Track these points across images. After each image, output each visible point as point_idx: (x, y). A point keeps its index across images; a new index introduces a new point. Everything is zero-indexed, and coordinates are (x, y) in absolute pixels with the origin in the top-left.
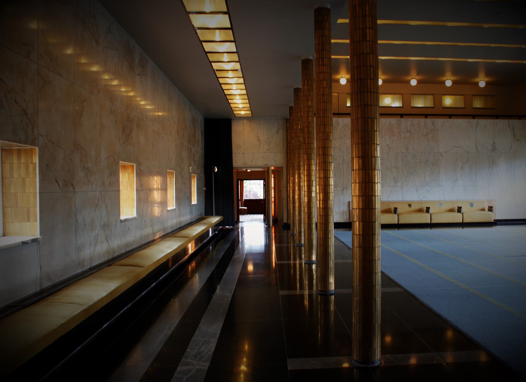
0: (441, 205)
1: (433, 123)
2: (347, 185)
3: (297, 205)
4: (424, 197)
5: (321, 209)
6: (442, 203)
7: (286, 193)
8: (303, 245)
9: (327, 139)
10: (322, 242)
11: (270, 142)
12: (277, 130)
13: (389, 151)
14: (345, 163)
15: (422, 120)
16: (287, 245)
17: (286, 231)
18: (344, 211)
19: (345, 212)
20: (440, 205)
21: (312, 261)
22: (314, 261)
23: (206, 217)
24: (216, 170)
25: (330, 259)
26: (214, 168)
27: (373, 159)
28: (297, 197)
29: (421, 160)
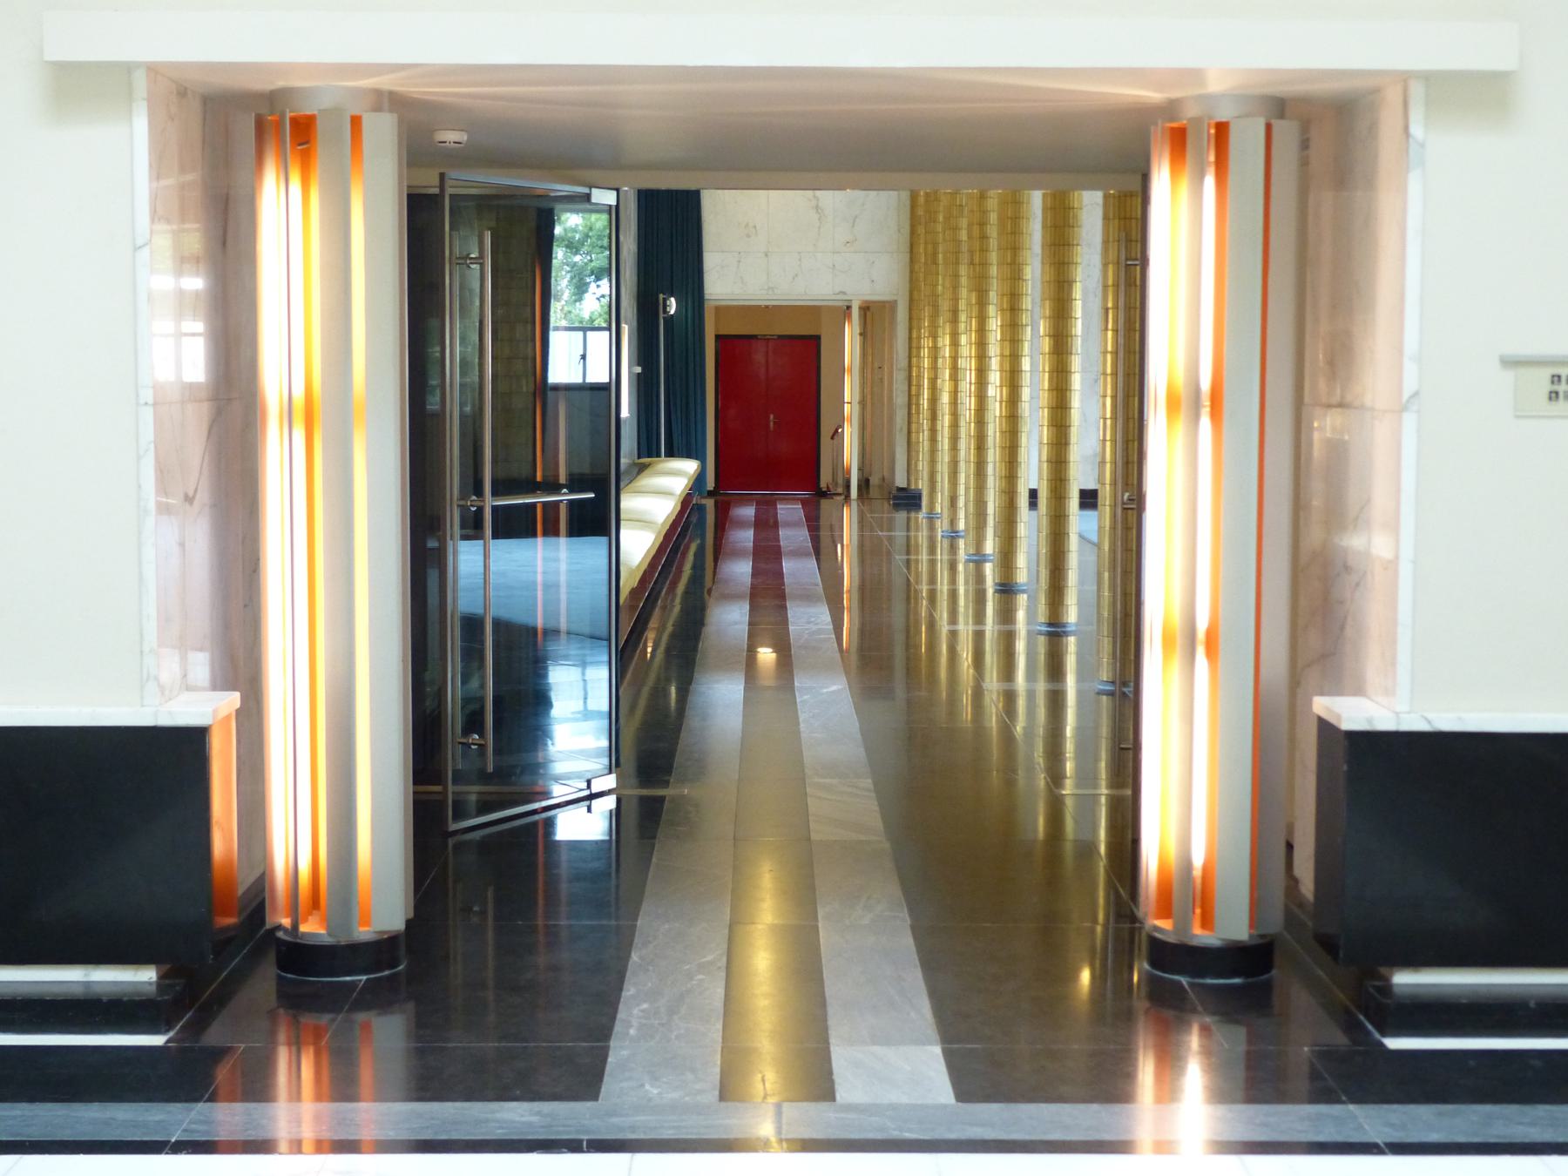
3: (945, 421)
5: (1004, 420)
7: (906, 388)
8: (963, 534)
9: (1019, 279)
10: (1003, 485)
11: (856, 217)
16: (906, 557)
17: (901, 516)
21: (984, 555)
22: (989, 555)
23: (643, 460)
24: (672, 312)
25: (1019, 520)
26: (665, 300)
27: (1069, 339)
28: (945, 398)
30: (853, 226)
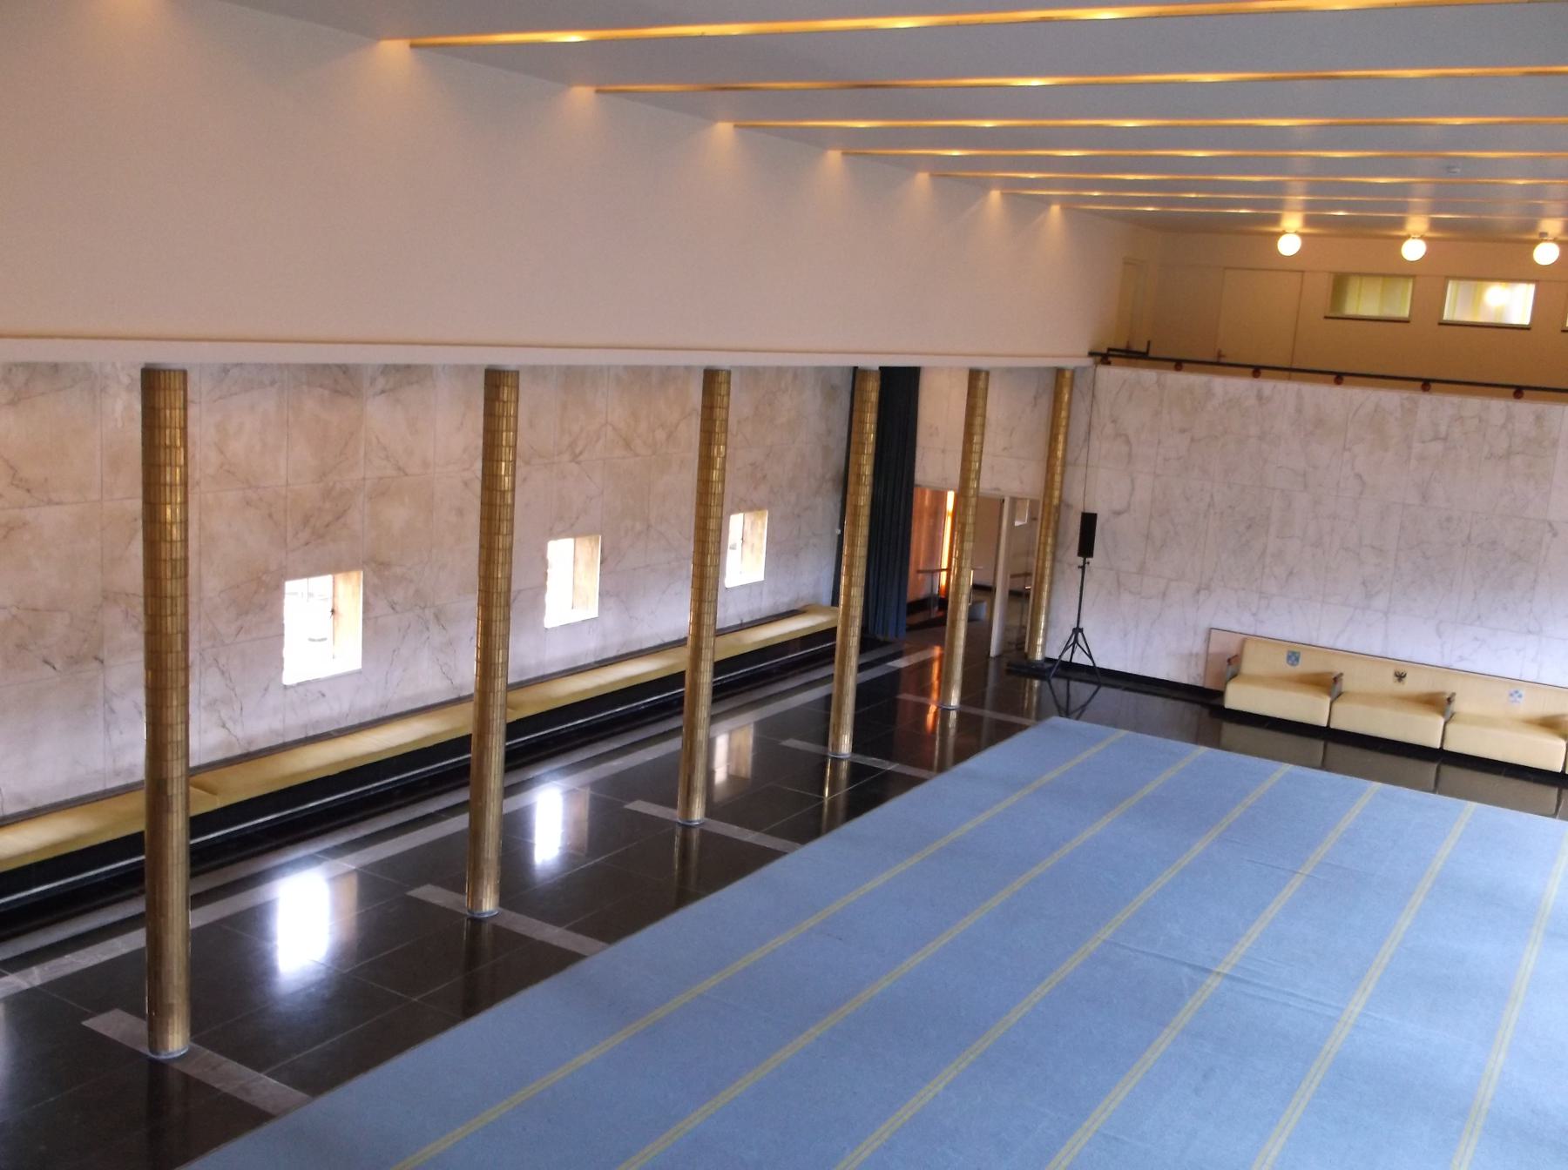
0: (1516, 695)
1: (1539, 418)
2: (1211, 579)
4: (1461, 659)
6: (1522, 692)
12: (1035, 398)
13: (1361, 493)
14: (1215, 513)
15: (1498, 407)
18: (1194, 651)
19: (1197, 655)
20: (1511, 695)
29: (1469, 537)
30: (1011, 435)
